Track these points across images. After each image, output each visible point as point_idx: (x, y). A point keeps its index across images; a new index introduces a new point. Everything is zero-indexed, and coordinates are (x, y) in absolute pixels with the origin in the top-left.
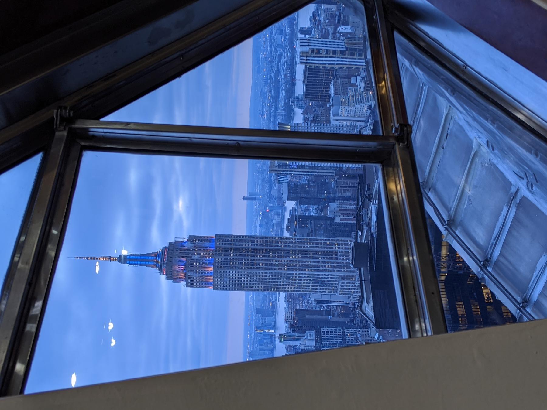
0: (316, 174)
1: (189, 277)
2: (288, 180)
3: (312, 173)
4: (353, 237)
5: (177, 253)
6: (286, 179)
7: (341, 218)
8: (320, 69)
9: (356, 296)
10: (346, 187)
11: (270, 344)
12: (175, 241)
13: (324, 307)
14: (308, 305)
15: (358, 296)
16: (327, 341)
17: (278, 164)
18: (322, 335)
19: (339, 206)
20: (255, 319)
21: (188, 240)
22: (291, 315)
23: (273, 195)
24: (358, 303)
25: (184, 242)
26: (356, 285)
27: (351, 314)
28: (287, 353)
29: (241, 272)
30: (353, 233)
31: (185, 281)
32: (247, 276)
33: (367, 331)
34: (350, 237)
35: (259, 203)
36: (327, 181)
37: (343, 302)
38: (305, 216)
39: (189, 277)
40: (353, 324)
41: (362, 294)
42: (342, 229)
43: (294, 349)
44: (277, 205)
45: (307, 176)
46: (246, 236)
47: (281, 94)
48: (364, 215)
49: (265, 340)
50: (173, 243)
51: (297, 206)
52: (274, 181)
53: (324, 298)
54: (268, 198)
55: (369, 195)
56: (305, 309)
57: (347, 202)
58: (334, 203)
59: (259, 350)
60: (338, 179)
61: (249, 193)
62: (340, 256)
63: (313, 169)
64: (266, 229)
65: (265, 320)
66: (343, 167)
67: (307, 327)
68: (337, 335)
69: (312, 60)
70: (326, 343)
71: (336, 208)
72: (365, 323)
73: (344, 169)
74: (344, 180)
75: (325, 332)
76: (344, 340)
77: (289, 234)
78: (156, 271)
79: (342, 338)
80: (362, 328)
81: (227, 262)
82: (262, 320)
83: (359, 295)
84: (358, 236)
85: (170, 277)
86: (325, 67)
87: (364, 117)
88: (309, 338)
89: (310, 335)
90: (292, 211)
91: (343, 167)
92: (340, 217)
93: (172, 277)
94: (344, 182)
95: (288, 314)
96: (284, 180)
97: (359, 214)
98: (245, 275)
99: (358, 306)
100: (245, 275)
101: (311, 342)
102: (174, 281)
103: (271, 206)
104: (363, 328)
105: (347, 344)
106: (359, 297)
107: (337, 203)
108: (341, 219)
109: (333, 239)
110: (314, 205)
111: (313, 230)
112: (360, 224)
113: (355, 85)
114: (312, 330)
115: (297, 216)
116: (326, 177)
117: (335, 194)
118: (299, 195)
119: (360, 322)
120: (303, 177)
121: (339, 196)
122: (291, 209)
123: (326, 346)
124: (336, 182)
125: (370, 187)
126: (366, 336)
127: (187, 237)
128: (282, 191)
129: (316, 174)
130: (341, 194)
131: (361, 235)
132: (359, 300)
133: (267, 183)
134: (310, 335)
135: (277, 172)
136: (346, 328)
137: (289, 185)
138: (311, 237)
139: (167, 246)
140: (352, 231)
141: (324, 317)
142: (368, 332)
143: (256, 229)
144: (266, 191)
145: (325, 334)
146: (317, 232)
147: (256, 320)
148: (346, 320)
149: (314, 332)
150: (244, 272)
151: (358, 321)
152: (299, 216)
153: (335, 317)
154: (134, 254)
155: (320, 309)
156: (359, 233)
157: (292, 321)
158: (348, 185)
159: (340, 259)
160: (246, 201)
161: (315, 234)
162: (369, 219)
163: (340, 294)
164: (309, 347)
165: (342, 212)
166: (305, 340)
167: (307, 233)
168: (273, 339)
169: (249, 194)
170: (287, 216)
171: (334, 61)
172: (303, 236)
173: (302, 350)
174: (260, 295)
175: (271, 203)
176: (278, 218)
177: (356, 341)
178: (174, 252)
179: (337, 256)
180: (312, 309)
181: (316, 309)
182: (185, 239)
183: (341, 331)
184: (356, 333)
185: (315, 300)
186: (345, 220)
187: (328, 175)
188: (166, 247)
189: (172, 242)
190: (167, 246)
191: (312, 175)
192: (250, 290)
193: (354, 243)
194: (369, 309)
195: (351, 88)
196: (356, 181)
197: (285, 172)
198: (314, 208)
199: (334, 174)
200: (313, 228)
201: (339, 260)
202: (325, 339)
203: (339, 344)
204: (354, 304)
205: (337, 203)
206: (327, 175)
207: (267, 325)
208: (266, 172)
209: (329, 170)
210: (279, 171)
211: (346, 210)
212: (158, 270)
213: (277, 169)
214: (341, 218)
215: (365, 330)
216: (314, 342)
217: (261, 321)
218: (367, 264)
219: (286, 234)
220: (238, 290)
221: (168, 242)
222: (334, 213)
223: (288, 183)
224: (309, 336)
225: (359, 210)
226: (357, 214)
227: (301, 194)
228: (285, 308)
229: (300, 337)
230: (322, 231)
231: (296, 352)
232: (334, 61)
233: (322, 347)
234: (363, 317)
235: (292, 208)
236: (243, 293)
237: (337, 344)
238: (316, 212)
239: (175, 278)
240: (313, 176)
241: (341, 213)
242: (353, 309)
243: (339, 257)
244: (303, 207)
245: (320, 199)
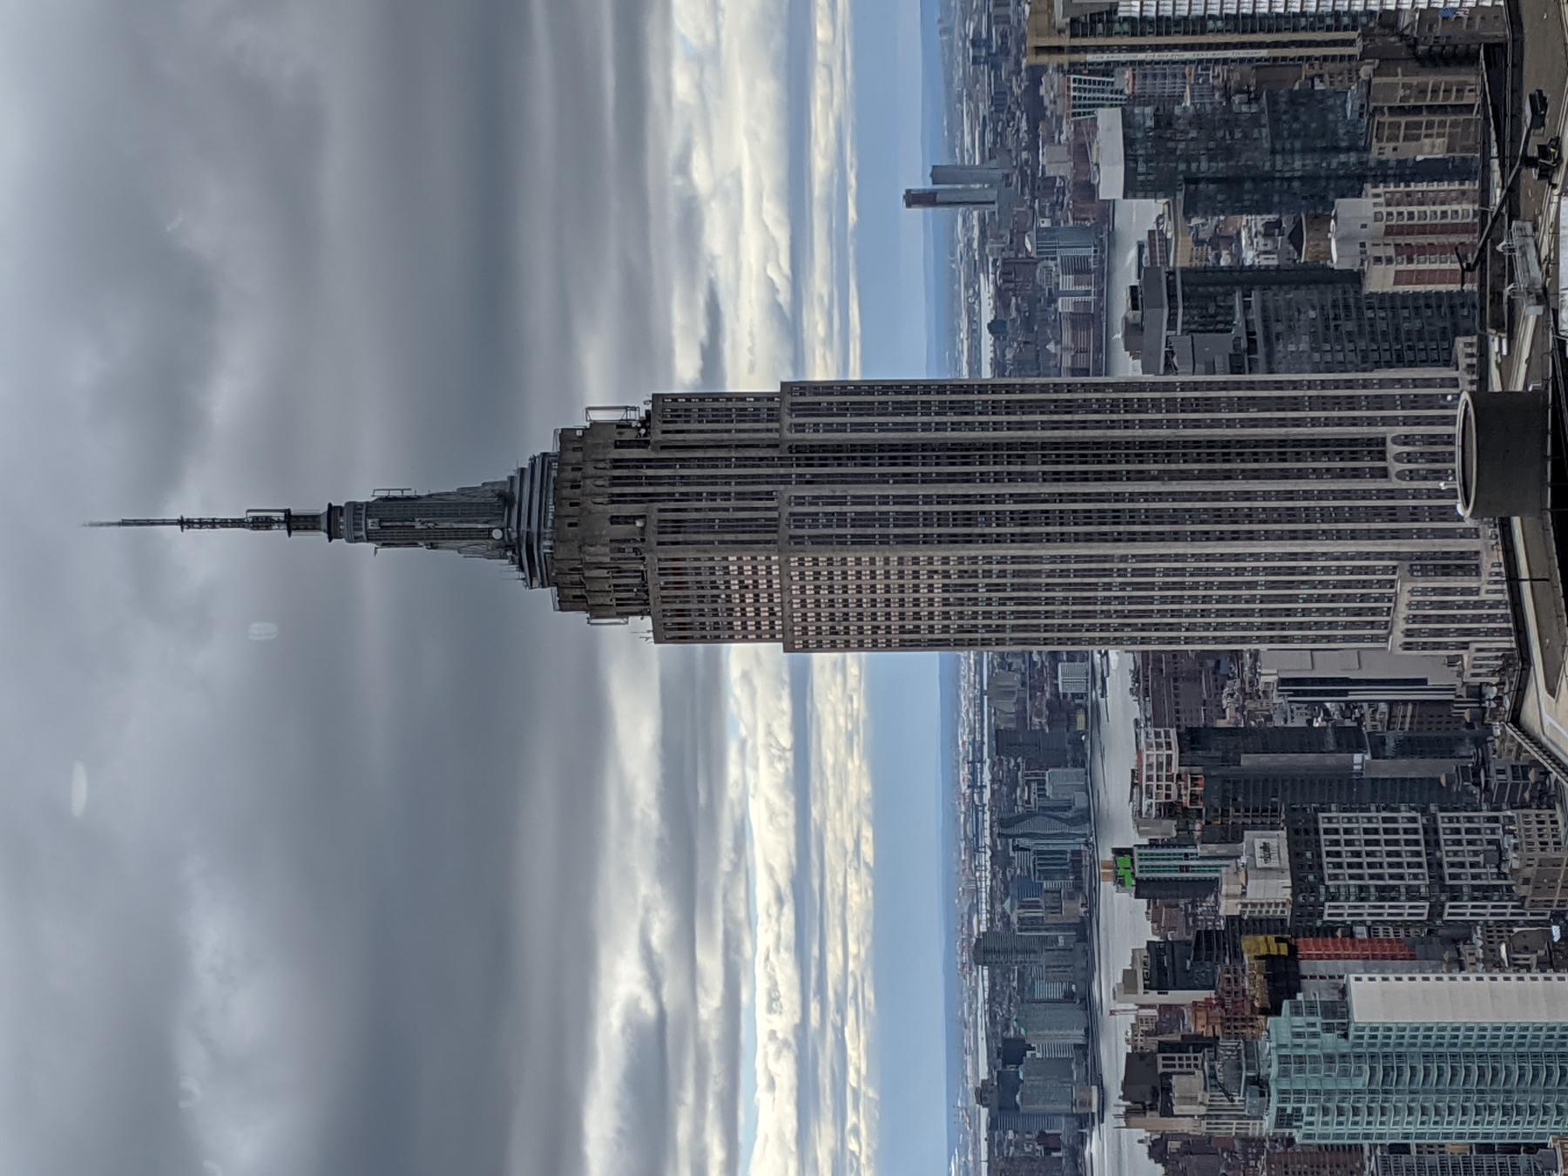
0: (1263, 53)
1: (665, 593)
2: (1122, 92)
3: (1242, 53)
4: (1463, 362)
5: (600, 482)
6: (1111, 92)
7: (1397, 272)
9: (1489, 650)
10: (1417, 110)
11: (1071, 897)
12: (588, 425)
13: (1327, 712)
14: (1250, 704)
15: (1498, 650)
16: (1352, 877)
17: (1068, 20)
18: (1324, 849)
19: (1384, 210)
20: (993, 781)
21: (647, 412)
22: (1169, 757)
23: (1050, 173)
24: (1496, 685)
25: (630, 426)
26: (1483, 596)
27: (1467, 741)
28: (1157, 939)
29: (916, 561)
30: (1460, 342)
31: (649, 614)
32: (944, 577)
33: (1548, 820)
34: (1447, 363)
35: (982, 220)
36: (1319, 86)
37: (1424, 681)
38: (1217, 269)
39: (665, 593)
40: (1476, 790)
41: (1518, 642)
42: (1406, 326)
43: (1190, 920)
44: (1071, 222)
45: (1218, 69)
46: (927, 387)
48: (1517, 254)
49: (1046, 879)
50: (579, 433)
51: (1171, 224)
52: (1055, 103)
53: (1330, 665)
54: (1027, 191)
55: (1543, 151)
56: (1237, 722)
57: (1423, 186)
58: (1359, 195)
59: (1020, 930)
60: (1377, 72)
61: (929, 171)
63: (1244, 32)
64: (1026, 343)
65: (1042, 783)
66: (1398, 10)
67: (1247, 810)
68: (1396, 842)
70: (1348, 886)
71: (1370, 223)
72: (1536, 783)
73: (1405, 21)
74: (1407, 80)
75: (1336, 831)
76: (1435, 865)
77: (1138, 362)
78: (505, 572)
79: (1423, 859)
80: (1522, 808)
81: (845, 513)
82: (1028, 783)
83: (1507, 645)
84: (1493, 358)
85: (575, 597)
88: (1260, 863)
89: (1265, 847)
90: (1146, 251)
91: (1398, 10)
92: (1393, 268)
93: (582, 597)
94: (1405, 86)
95: (1154, 752)
96: (1101, 95)
97: (1494, 251)
98: (936, 572)
99: (1499, 699)
100: (931, 574)
101: (1269, 881)
102: (597, 617)
103: (1046, 229)
104: (1529, 807)
105: (1451, 886)
106: (1506, 657)
107: (1377, 196)
108: (1399, 278)
109: (1361, 376)
110: (1259, 213)
111: (1259, 337)
112: (1501, 295)
114: (1274, 827)
115: (1172, 273)
116: (1317, 66)
117: (1367, 149)
118: (1182, 166)
119: (1514, 778)
120: (1197, 76)
121: (1383, 158)
122: (1144, 237)
123: (1347, 899)
124: (1364, 90)
125: (1544, 106)
126: (1546, 843)
127: (645, 403)
128: (1094, 153)
129: (1263, 53)
130: (1395, 149)
131: (1505, 352)
132: (1502, 671)
133: (1018, 113)
134: (1265, 847)
135: (1064, 59)
136: (1442, 810)
137: (1127, 124)
138: (1251, 371)
139: (551, 446)
140: (1456, 334)
141: (1330, 760)
142: (1555, 822)
143: (975, 348)
144: (1014, 154)
145: (1337, 843)
146: (1280, 347)
147: (996, 787)
148: (1441, 769)
149: (1283, 833)
150: (930, 561)
151: (1500, 772)
152: (1184, 271)
153: (1385, 758)
154: (398, 494)
155: (1310, 722)
156: (1496, 345)
157: (1174, 786)
158: (1428, 102)
159: (1400, 475)
160: (918, 211)
161: (1270, 355)
162: (1547, 271)
163: (1408, 646)
164: (1262, 905)
165: (1401, 240)
166: (1243, 874)
167: (1230, 355)
168: (1085, 875)
169: (932, 175)
172: (1207, 373)
173: (1230, 919)
174: (1010, 665)
175: (1043, 215)
176: (1083, 288)
177: (1495, 870)
178: (584, 478)
179: (1384, 459)
180: (1269, 725)
181: (1289, 724)
182: (634, 409)
183: (1419, 825)
184: (1493, 831)
185: (1283, 681)
186: (1420, 277)
187: (1325, 58)
188: (544, 454)
189: (575, 430)
190: (551, 446)
191: (1242, 60)
192: (959, 644)
193: (1472, 394)
196: (1472, 79)
197: (1106, 57)
198: (1262, 229)
199: (1355, 50)
200: (1258, 329)
201: (1394, 479)
202: (1339, 866)
203: (1408, 887)
204: (1477, 693)
205: (1377, 196)
206: (1317, 59)
207: (1052, 809)
208: (1012, 59)
209: (1329, 29)
210: (1074, 50)
211: (1423, 230)
212: (514, 567)
213: (1065, 41)
214: (1397, 272)
215: (1537, 816)
216: (1288, 882)
217: (1023, 791)
218: (1543, 501)
219: (1128, 367)
220: (904, 645)
221: (555, 431)
222: (1363, 245)
223: (1123, 112)
224: (1259, 852)
225: (1491, 225)
226: (1483, 250)
227: (1188, 163)
228: (1137, 722)
229: (1217, 862)
230: (1306, 338)
231: (1199, 932)
233: (1327, 904)
234: (1526, 751)
235: (1151, 233)
236: (931, 660)
237: (1403, 890)
238: (1269, 248)
239: (601, 601)
240: (1246, 68)
241: (1397, 245)
242: (1472, 714)
244: (1203, 225)
245: (1283, 179)
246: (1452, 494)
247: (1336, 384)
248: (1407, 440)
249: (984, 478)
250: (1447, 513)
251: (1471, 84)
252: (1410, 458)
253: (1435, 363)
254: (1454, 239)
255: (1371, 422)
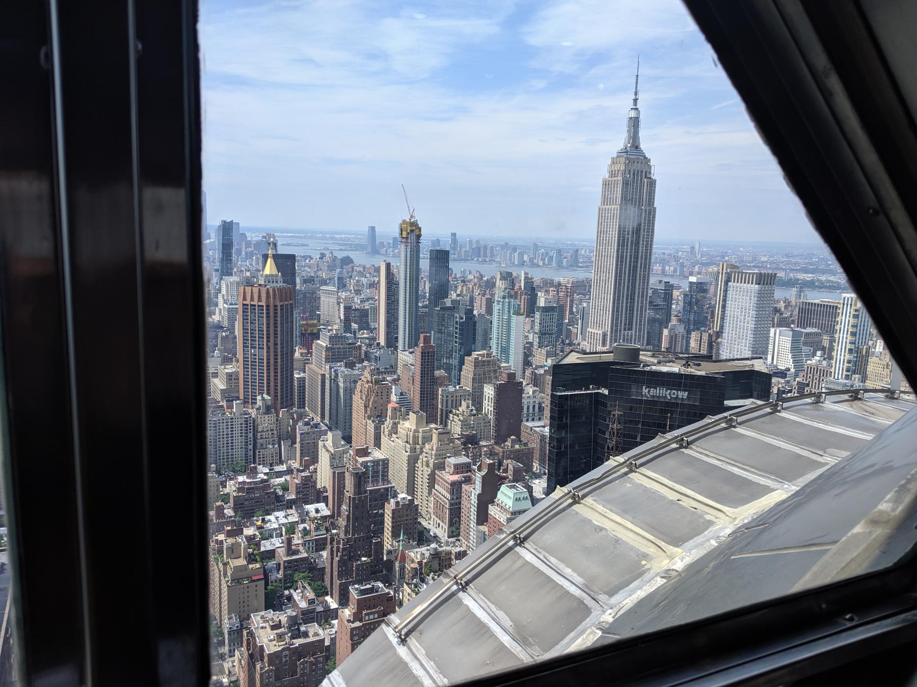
8: (835, 318)
10: (701, 341)
30: (652, 347)
47: (810, 275)
60: (710, 334)
62: (628, 333)
69: (847, 310)
86: (837, 324)
87: (777, 362)
113: (814, 354)
135: (721, 271)
152: (672, 293)
163: (589, 332)
170: (672, 281)
171: (843, 334)
194: (573, 359)
195: (812, 351)
213: (724, 271)
232: (843, 334)
243: (626, 332)
246: (619, 342)
247: (645, 322)
248: (632, 335)
249: (631, 249)
250: (615, 341)
251: (704, 351)
252: (628, 336)
253: (647, 341)
254: (673, 347)
255: (636, 328)
